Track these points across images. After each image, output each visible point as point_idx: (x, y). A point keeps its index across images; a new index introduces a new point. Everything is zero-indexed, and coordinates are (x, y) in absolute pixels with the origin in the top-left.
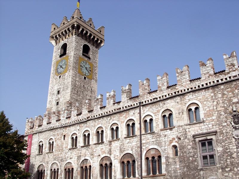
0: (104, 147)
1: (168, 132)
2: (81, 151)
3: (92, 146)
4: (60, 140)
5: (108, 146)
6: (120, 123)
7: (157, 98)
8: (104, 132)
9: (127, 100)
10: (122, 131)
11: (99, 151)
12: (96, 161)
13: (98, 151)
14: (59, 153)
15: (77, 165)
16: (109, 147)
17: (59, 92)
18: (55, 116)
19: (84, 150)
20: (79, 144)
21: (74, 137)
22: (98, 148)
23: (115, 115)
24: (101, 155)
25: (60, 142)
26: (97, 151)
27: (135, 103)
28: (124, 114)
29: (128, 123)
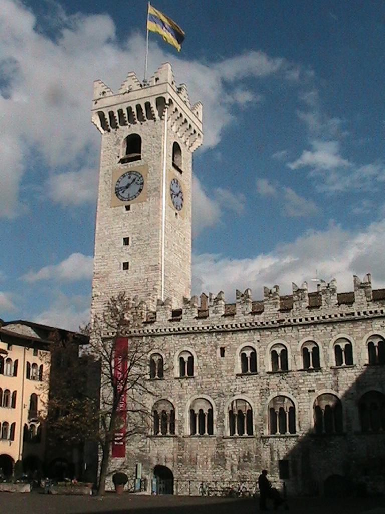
0: (321, 377)
2: (268, 381)
3: (293, 373)
4: (211, 355)
5: (331, 376)
6: (355, 338)
8: (321, 350)
9: (368, 301)
10: (359, 354)
11: (312, 383)
12: (306, 400)
13: (310, 383)
14: (210, 380)
15: (259, 404)
16: (333, 377)
17: (126, 241)
18: (189, 307)
19: (275, 380)
20: (262, 368)
21: (248, 353)
22: (308, 377)
24: (316, 391)
25: (211, 360)
26: (306, 383)
28: (363, 326)
29: (370, 341)
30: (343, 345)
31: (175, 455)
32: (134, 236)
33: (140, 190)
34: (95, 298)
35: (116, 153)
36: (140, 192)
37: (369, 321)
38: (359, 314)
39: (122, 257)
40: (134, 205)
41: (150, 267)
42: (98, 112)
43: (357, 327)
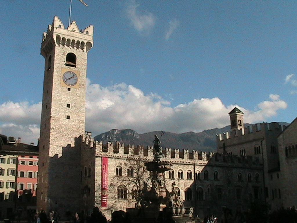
1: (207, 182)
5: (177, 181)
7: (202, 164)
17: (68, 106)
22: (171, 181)
23: (181, 165)
27: (192, 162)
28: (186, 166)
30: (180, 172)
31: (127, 206)
32: (72, 104)
33: (76, 83)
34: (52, 129)
35: (63, 59)
36: (76, 84)
37: (188, 165)
38: (185, 162)
39: (67, 112)
40: (73, 89)
41: (80, 121)
42: (57, 35)
43: (184, 167)
